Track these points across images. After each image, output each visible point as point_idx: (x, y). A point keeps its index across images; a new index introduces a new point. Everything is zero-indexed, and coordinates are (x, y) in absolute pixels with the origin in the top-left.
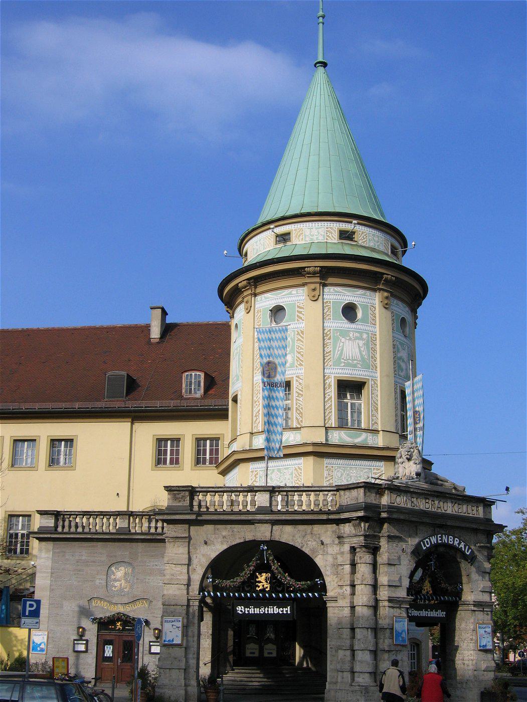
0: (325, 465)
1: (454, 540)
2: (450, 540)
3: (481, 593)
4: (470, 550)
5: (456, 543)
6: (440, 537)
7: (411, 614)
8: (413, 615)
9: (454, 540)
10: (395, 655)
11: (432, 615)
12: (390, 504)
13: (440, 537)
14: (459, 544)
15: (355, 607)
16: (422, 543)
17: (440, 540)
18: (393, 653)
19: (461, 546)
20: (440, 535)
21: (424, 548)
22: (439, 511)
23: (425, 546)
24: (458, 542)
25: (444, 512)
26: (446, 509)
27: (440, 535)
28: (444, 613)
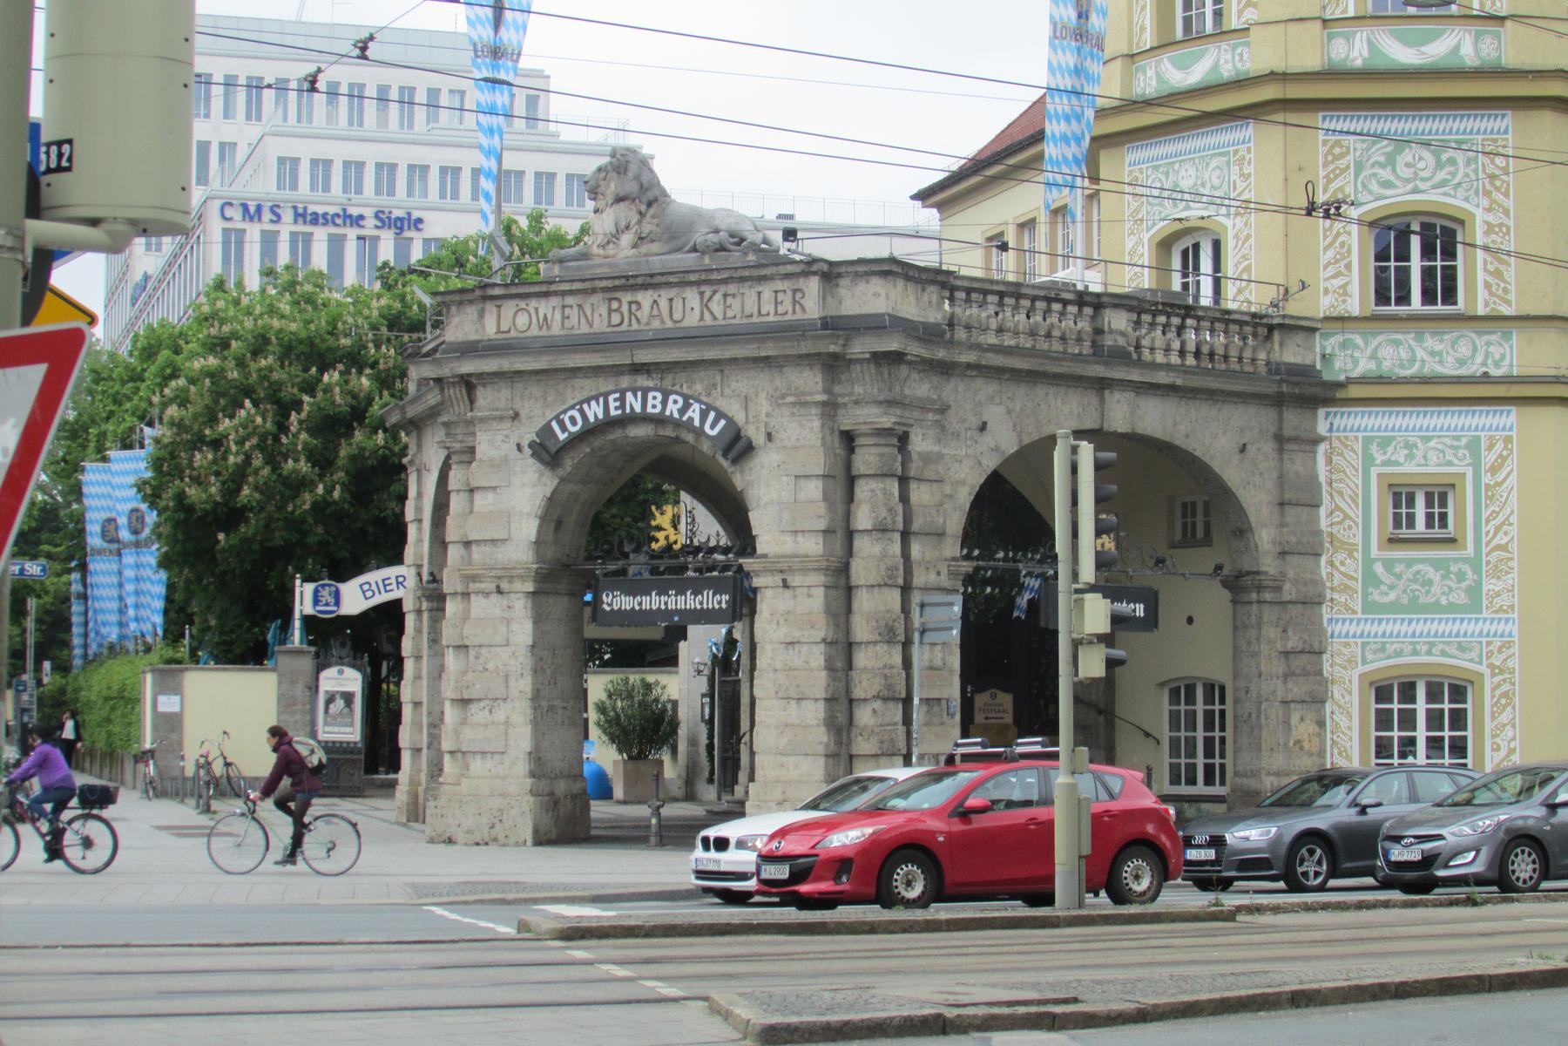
0: (1127, 169)
1: (664, 403)
2: (650, 402)
3: (788, 538)
4: (722, 422)
5: (673, 409)
6: (615, 400)
7: (610, 605)
8: (616, 608)
9: (664, 403)
10: (487, 710)
11: (681, 606)
12: (497, 336)
13: (615, 400)
14: (682, 411)
15: (469, 594)
16: (554, 425)
17: (616, 408)
18: (482, 704)
19: (689, 413)
20: (617, 395)
21: (562, 436)
22: (656, 324)
23: (564, 428)
24: (680, 404)
25: (669, 324)
26: (677, 315)
27: (617, 395)
28: (725, 597)
